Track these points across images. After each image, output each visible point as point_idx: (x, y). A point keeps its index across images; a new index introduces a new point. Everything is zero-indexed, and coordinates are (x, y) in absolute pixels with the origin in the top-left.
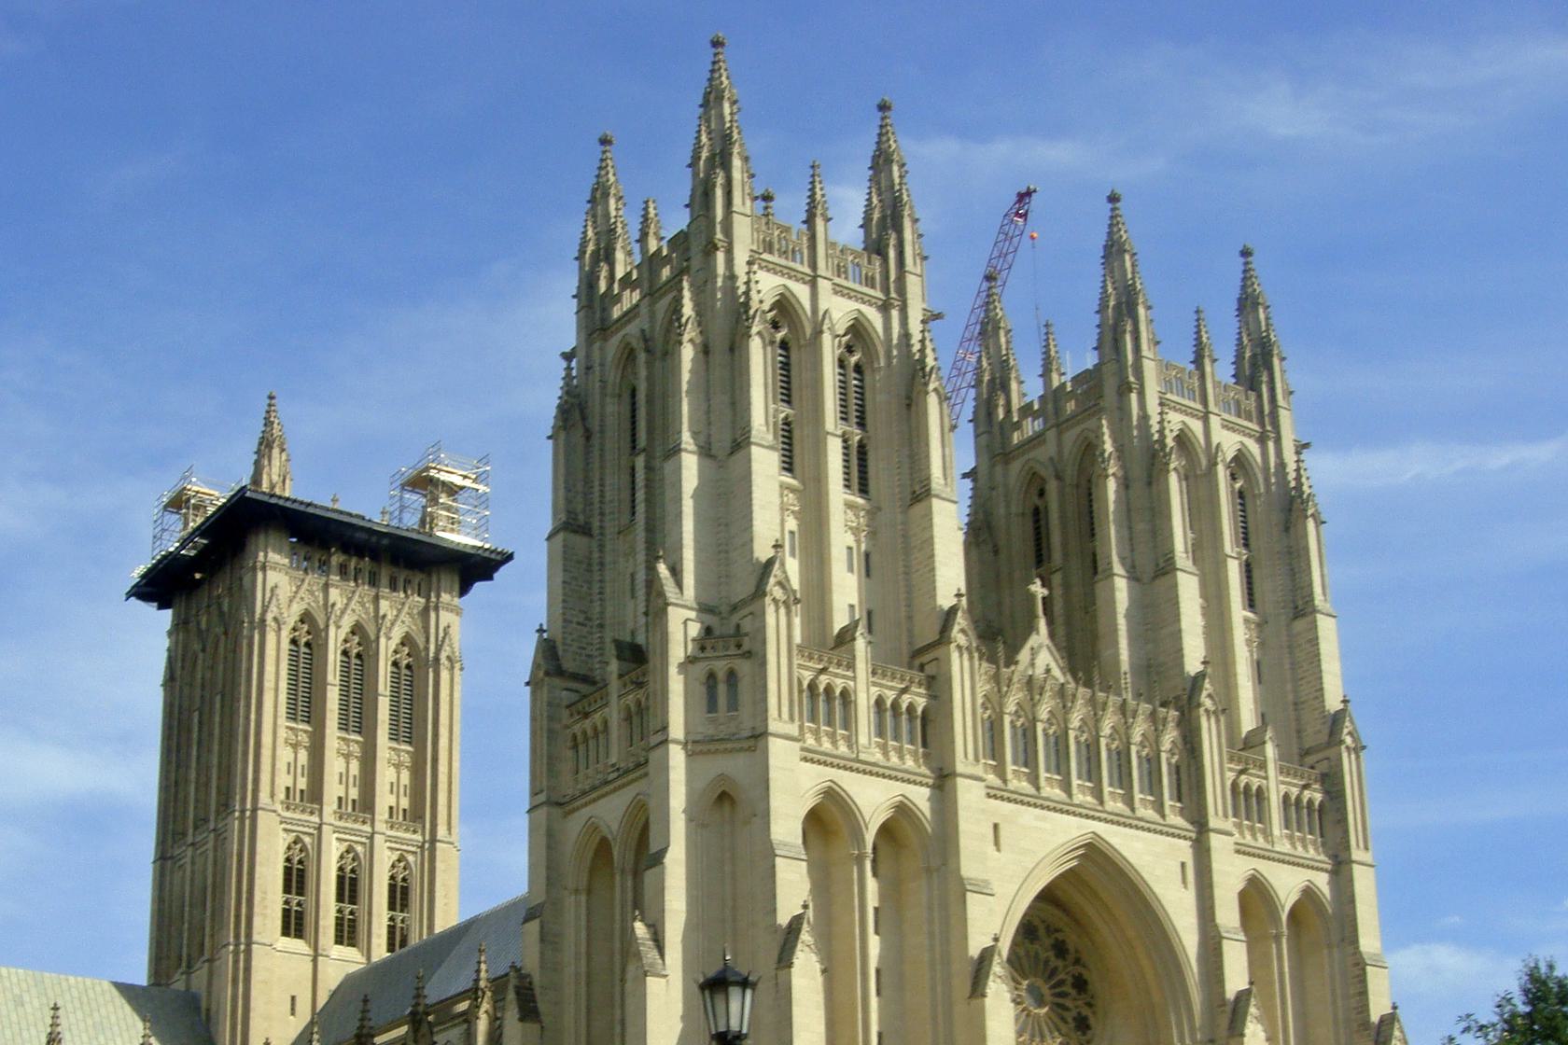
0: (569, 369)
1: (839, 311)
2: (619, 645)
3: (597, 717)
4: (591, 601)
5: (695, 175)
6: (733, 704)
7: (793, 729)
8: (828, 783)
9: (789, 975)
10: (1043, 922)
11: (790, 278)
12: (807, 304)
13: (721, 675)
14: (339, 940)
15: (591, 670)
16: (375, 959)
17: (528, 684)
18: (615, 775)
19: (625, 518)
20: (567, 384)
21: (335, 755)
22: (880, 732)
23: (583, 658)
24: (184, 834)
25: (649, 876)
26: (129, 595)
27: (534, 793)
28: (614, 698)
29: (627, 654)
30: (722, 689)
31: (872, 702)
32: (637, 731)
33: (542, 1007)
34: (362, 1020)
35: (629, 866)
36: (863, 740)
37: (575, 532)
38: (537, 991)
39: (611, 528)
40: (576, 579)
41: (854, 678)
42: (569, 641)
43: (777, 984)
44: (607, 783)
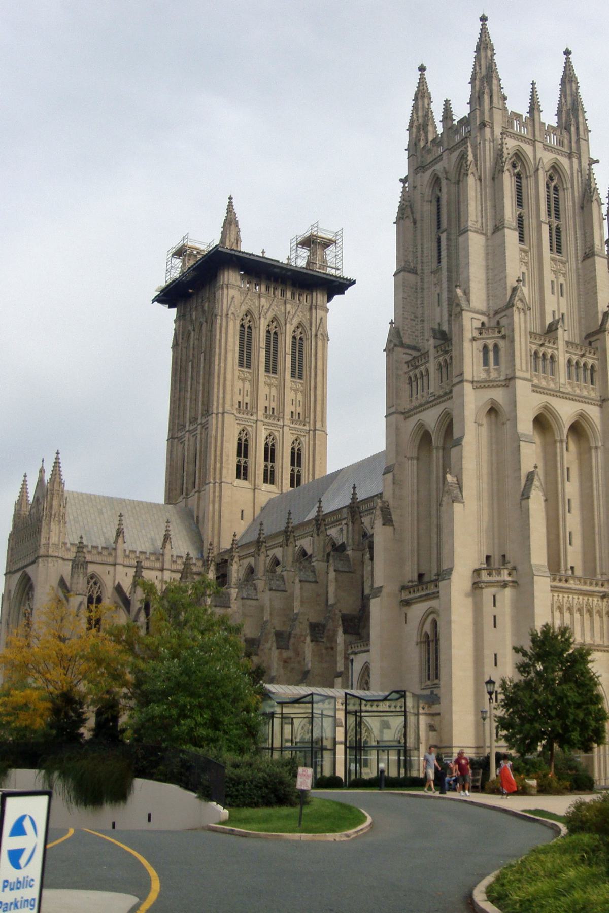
0: (404, 187)
1: (547, 158)
2: (433, 330)
3: (423, 368)
4: (417, 308)
5: (473, 88)
7: (528, 376)
8: (580, 411)
9: (528, 502)
11: (522, 141)
13: (491, 347)
14: (265, 481)
15: (417, 343)
16: (284, 491)
17: (384, 350)
18: (433, 398)
19: (434, 265)
20: (403, 195)
21: (290, 390)
22: (570, 378)
23: (414, 337)
24: (184, 426)
25: (454, 452)
26: (153, 301)
27: (388, 407)
28: (432, 358)
29: (438, 336)
30: (491, 354)
31: (566, 361)
32: (444, 376)
33: (394, 518)
34: (288, 523)
35: (440, 445)
36: (562, 381)
37: (409, 272)
38: (392, 510)
39: (427, 271)
40: (409, 296)
41: (557, 349)
42: (406, 328)
43: (521, 507)
44: (429, 402)
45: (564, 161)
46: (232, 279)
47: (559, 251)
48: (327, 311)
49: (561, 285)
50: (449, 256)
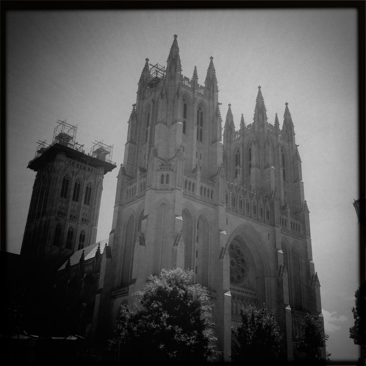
0: (134, 108)
1: (199, 98)
6: (167, 182)
10: (235, 245)
12: (192, 96)
17: (117, 177)
26: (28, 167)
27: (116, 203)
45: (206, 101)
46: (61, 157)
47: (201, 140)
48: (103, 177)
49: (201, 154)
50: (151, 136)
